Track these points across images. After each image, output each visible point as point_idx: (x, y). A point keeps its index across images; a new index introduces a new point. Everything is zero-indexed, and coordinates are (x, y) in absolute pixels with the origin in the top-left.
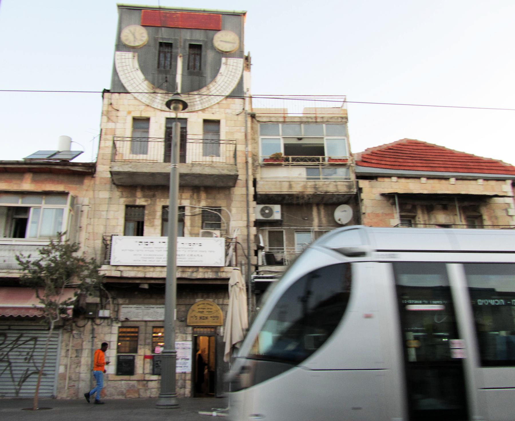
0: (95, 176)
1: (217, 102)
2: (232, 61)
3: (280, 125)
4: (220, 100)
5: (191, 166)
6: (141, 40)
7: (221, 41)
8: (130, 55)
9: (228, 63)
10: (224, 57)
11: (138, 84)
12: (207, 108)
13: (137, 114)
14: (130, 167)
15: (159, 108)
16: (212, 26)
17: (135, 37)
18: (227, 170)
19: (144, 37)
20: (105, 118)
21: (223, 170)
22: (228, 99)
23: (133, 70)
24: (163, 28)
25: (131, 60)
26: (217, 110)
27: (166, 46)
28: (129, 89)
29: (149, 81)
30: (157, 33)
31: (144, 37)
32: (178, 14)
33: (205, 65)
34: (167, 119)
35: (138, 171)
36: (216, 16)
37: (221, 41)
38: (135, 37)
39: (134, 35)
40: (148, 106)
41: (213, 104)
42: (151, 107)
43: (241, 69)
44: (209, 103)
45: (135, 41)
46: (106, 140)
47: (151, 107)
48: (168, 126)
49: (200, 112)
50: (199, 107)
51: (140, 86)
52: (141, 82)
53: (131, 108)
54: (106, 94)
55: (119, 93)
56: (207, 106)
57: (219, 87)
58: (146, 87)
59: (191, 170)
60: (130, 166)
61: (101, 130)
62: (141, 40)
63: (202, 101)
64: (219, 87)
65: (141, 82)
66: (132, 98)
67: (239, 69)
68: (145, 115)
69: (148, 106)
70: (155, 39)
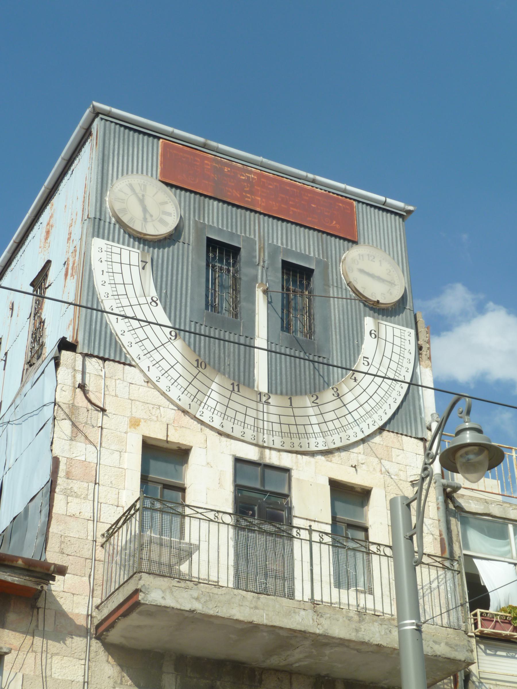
0: (40, 603)
1: (361, 436)
2: (390, 329)
3: (511, 527)
4: (367, 432)
5: (356, 618)
6: (162, 222)
7: (362, 271)
8: (133, 254)
9: (382, 335)
10: (369, 316)
11: (157, 344)
12: (339, 449)
13: (157, 433)
14: (197, 599)
15: (216, 424)
16: (334, 226)
17: (145, 210)
18: (447, 644)
19: (169, 214)
20: (64, 427)
21: (435, 642)
22: (385, 433)
23: (142, 300)
24: (216, 203)
25: (135, 270)
26: (361, 458)
27: (222, 252)
28: (134, 352)
29: (184, 340)
30: (201, 210)
31: (169, 214)
32: (251, 172)
33: (326, 328)
34: (238, 461)
35: (219, 614)
36: (342, 202)
37: (362, 271)
38: (145, 210)
39: (142, 201)
40: (185, 412)
41: (353, 440)
42: (195, 418)
43: (412, 357)
44: (342, 434)
45: (145, 219)
46: (68, 493)
47: (195, 418)
48: (240, 482)
49: (320, 458)
50: (317, 443)
51: (162, 350)
52: (164, 340)
53: (139, 413)
54: (66, 355)
55: (104, 359)
56: (338, 444)
57: (364, 398)
58: (179, 358)
59: (357, 631)
60: (195, 595)
61: (56, 461)
62: (162, 222)
63: (324, 427)
64: (364, 398)
65: (164, 340)
66: (140, 379)
67: (407, 355)
68: (177, 437)
69: (185, 412)
70: (200, 228)
